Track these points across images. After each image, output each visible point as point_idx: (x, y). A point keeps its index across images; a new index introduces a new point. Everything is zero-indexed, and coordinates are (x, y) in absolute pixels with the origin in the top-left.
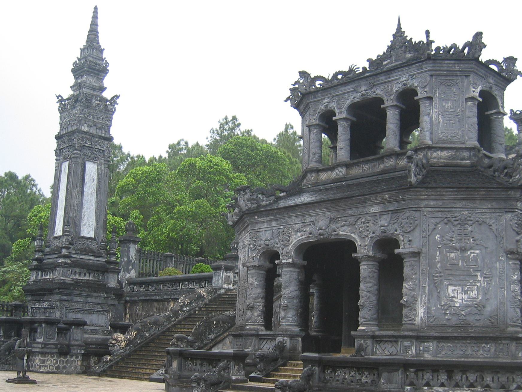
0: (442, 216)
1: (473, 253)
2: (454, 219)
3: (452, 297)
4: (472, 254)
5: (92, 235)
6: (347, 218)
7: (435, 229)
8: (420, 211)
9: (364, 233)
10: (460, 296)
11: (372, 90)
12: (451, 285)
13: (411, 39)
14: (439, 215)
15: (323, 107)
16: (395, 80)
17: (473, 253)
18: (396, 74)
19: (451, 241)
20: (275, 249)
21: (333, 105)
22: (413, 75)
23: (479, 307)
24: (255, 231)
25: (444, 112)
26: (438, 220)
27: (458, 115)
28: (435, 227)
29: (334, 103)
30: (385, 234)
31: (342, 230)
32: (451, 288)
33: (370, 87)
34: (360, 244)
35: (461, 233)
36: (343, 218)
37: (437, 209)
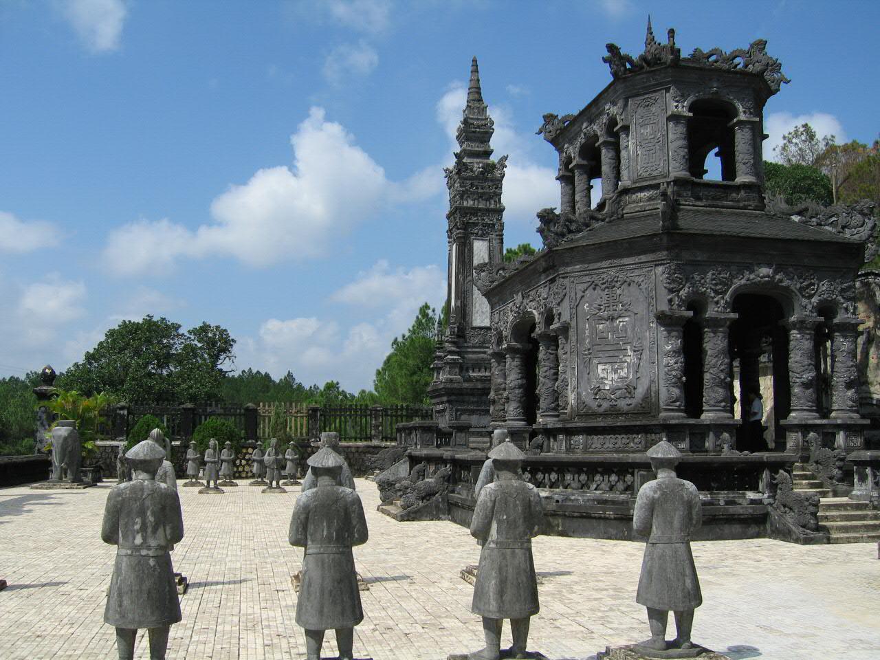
1: (623, 321)
3: (602, 378)
4: (621, 323)
5: (487, 323)
7: (583, 296)
10: (610, 378)
17: (623, 321)
23: (630, 390)
26: (585, 286)
28: (583, 294)
32: (601, 367)
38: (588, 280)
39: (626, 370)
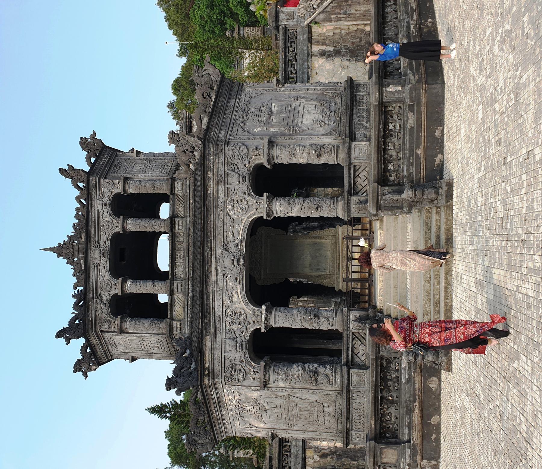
0: (237, 127)
1: (275, 107)
2: (241, 119)
4: (275, 107)
6: (225, 228)
7: (248, 132)
8: (228, 141)
9: (244, 205)
14: (235, 129)
15: (104, 310)
16: (99, 217)
17: (275, 107)
18: (93, 214)
19: (261, 121)
21: (106, 297)
22: (99, 195)
24: (223, 371)
25: (144, 171)
26: (240, 130)
27: (150, 162)
31: (237, 236)
33: (99, 247)
34: (255, 210)
35: (256, 115)
36: (225, 235)
37: (230, 130)
38: (236, 128)
39: (310, 106)
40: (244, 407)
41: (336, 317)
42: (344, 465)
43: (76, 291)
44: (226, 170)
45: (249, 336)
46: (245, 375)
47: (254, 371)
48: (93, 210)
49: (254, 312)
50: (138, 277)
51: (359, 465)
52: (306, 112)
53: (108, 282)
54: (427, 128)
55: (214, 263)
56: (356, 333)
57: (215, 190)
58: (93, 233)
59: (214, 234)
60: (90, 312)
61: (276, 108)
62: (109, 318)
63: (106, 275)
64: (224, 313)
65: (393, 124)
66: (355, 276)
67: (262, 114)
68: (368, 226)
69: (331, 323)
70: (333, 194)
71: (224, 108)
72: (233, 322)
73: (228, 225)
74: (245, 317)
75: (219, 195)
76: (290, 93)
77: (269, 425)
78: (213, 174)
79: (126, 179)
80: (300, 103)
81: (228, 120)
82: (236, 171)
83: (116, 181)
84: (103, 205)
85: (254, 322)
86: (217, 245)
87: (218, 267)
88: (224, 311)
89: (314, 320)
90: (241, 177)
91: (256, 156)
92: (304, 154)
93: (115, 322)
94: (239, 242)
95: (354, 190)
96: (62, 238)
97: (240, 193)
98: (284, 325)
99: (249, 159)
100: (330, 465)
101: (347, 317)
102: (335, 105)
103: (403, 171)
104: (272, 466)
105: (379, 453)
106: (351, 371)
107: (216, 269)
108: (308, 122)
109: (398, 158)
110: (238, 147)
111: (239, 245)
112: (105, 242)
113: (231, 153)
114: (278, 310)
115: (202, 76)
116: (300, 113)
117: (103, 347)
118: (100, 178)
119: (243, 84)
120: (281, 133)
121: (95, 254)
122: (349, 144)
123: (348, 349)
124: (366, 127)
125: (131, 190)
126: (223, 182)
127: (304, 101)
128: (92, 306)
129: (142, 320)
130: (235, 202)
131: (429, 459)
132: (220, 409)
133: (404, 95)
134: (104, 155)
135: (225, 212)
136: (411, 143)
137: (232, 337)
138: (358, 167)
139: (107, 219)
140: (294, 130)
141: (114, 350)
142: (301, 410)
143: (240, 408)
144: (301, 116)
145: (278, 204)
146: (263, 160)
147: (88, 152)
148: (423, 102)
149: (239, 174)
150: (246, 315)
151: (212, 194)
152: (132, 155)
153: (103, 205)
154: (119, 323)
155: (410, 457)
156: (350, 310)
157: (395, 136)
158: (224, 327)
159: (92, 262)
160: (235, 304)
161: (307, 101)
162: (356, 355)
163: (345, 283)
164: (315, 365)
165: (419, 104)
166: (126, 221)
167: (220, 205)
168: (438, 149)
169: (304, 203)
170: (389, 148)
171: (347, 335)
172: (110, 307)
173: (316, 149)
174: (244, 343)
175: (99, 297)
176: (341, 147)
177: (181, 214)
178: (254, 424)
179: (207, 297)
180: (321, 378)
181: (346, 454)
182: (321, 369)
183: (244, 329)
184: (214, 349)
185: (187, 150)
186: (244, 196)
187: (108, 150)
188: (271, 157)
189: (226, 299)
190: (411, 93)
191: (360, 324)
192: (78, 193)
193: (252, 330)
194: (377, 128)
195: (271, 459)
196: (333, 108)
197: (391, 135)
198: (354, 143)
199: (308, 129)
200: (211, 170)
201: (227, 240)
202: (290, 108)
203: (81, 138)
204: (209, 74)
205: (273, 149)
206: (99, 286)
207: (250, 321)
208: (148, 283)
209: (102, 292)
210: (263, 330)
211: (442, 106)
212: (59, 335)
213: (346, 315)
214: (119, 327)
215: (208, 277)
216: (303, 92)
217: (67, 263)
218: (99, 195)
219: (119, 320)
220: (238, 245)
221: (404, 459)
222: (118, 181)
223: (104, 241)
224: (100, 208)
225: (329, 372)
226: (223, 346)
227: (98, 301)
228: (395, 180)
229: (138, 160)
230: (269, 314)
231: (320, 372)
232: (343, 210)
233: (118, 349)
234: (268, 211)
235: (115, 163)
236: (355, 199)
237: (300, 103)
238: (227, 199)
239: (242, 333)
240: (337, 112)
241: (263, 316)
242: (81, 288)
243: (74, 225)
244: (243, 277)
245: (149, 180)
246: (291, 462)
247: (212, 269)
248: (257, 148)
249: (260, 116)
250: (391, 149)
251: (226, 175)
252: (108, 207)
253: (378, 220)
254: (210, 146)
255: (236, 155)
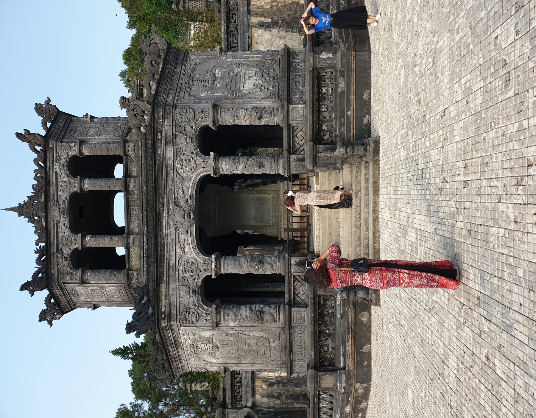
1: (218, 74)
2: (187, 85)
4: (218, 73)
6: (175, 186)
7: (194, 96)
9: (192, 164)
11: (61, 204)
12: (244, 86)
13: (28, 196)
14: (182, 94)
16: (57, 178)
17: (218, 74)
18: (51, 176)
19: (206, 86)
20: (200, 283)
21: (67, 251)
24: (178, 314)
25: (98, 135)
26: (187, 94)
27: (103, 126)
29: (64, 251)
30: (194, 138)
31: (187, 192)
33: (58, 205)
34: (202, 169)
36: (176, 192)
38: (183, 93)
39: (250, 72)
40: (198, 346)
41: (279, 262)
42: (289, 391)
43: (38, 247)
44: (174, 132)
45: (200, 282)
46: (198, 317)
47: (206, 314)
48: (51, 171)
49: (205, 261)
50: (96, 232)
51: (302, 391)
52: (248, 77)
53: (69, 237)
54: (356, 91)
55: (166, 217)
56: (296, 276)
57: (164, 151)
58: (52, 193)
59: (165, 191)
60: (52, 266)
61: (219, 74)
62: (71, 271)
63: (66, 231)
64: (177, 263)
65: (326, 88)
66: (295, 226)
67: (206, 79)
68: (306, 181)
69: (274, 268)
70: (274, 154)
71: (172, 75)
72: (185, 271)
73: (178, 182)
74: (196, 266)
75: (169, 155)
76: (232, 60)
77: (221, 361)
78: (162, 136)
79: (82, 143)
80: (242, 69)
81: (175, 85)
82: (183, 132)
83: (73, 144)
84: (61, 167)
85: (205, 270)
86: (168, 201)
87: (170, 222)
88: (177, 261)
89: (259, 266)
90: (188, 138)
91: (202, 118)
92: (246, 116)
93: (76, 274)
94: (189, 198)
95: (293, 149)
96: (22, 199)
97: (188, 153)
98: (233, 272)
99: (195, 122)
100: (277, 393)
101: (289, 262)
102: (273, 71)
103: (336, 131)
104: (226, 396)
105: (318, 379)
106: (293, 309)
107: (168, 223)
108: (249, 87)
109: (331, 119)
110: (185, 111)
111: (189, 201)
112: (64, 201)
113: (178, 116)
114: (227, 259)
115: (150, 45)
116: (242, 78)
117: (66, 297)
118: (56, 141)
119: (188, 53)
120: (224, 97)
121: (55, 213)
122: (287, 106)
123: (290, 290)
124: (302, 92)
125: (86, 153)
126: (172, 143)
127: (245, 68)
128: (54, 260)
129: (102, 272)
130: (184, 161)
131: (362, 383)
132: (177, 348)
133: (335, 61)
134: (59, 119)
135: (175, 171)
136: (342, 104)
137: (185, 284)
138: (295, 128)
139: (65, 180)
140: (236, 94)
141: (76, 299)
142: (249, 346)
143: (194, 347)
144: (242, 81)
145: (224, 163)
146: (208, 122)
147: (43, 117)
148: (352, 68)
149: (187, 136)
150: (198, 264)
151: (162, 154)
152: (86, 120)
153: (61, 167)
154: (80, 275)
155: (346, 381)
156: (291, 256)
157: (328, 98)
158: (177, 275)
159: (52, 220)
160: (187, 254)
161: (248, 68)
162: (297, 295)
163: (286, 233)
164: (261, 306)
165: (349, 69)
166: (83, 181)
167: (169, 165)
168: (365, 110)
169: (248, 161)
170: (323, 110)
171: (289, 278)
172: (71, 261)
173: (257, 112)
174: (196, 289)
175: (60, 252)
176: (280, 109)
177: (134, 174)
178: (207, 360)
179: (161, 249)
180: (266, 317)
181: (290, 382)
182: (267, 309)
183: (196, 276)
184: (168, 296)
185: (138, 114)
186: (192, 155)
187: (63, 115)
188: (216, 119)
189: (178, 250)
190: (342, 60)
191: (300, 268)
192: (35, 156)
193: (204, 277)
194: (312, 92)
195: (224, 390)
196: (272, 74)
197: (325, 99)
198: (291, 106)
199: (250, 93)
200: (161, 132)
201: (177, 197)
202: (232, 74)
203: (36, 104)
204: (156, 43)
205: (217, 112)
206: (60, 241)
207: (201, 269)
208: (106, 238)
209: (63, 247)
210: (213, 277)
211: (369, 71)
212: (24, 287)
213: (288, 261)
214: (80, 279)
215: (161, 231)
216: (244, 59)
217: (28, 222)
218: (56, 158)
219: (80, 272)
220: (187, 201)
221: (340, 383)
222: (74, 144)
223: (63, 200)
224: (57, 170)
225: (273, 311)
226: (178, 292)
227: (59, 255)
228: (328, 139)
229: (92, 124)
230: (219, 262)
231: (265, 312)
232: (284, 168)
233: (81, 299)
234: (215, 170)
235: (70, 128)
236: (293, 157)
237: (242, 69)
238: (176, 159)
239: (194, 280)
240: (276, 78)
241: (213, 264)
242: (43, 244)
243: (33, 186)
244: (193, 230)
245: (104, 143)
246: (242, 392)
247: (165, 223)
248: (202, 111)
249: (204, 82)
250: (324, 111)
251: (174, 136)
252: (65, 169)
253: (314, 175)
254: (159, 110)
255: (183, 117)
